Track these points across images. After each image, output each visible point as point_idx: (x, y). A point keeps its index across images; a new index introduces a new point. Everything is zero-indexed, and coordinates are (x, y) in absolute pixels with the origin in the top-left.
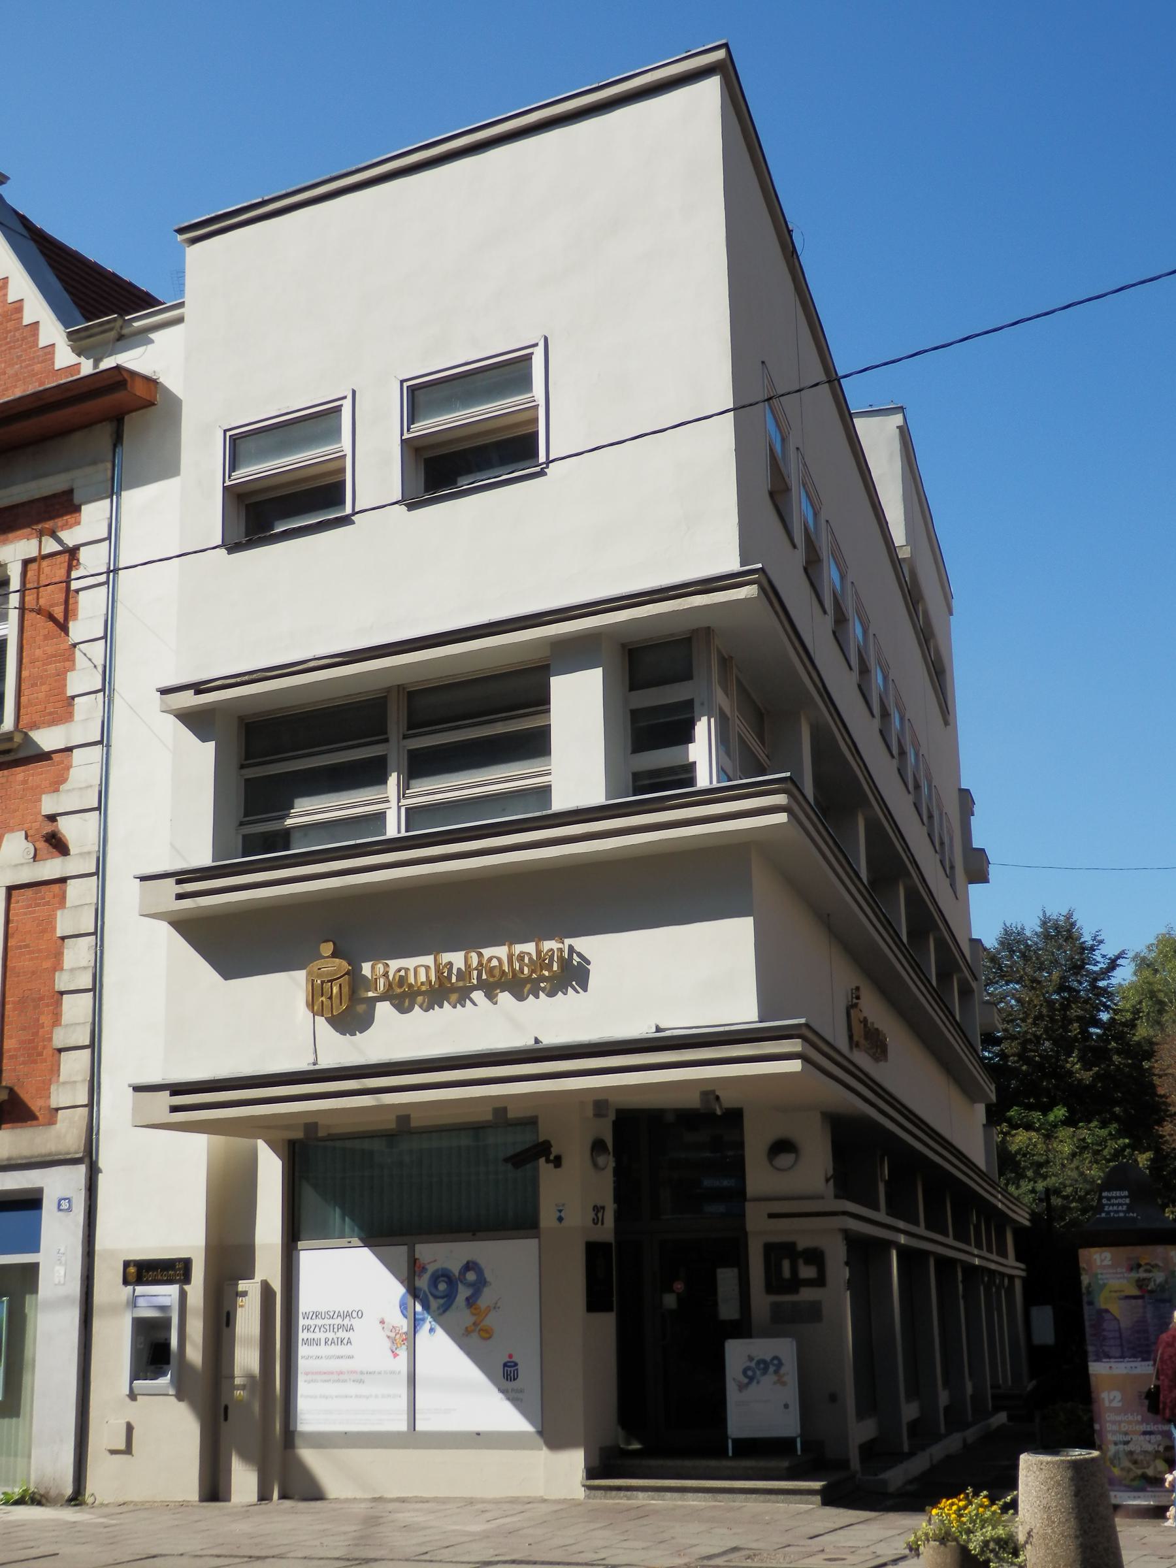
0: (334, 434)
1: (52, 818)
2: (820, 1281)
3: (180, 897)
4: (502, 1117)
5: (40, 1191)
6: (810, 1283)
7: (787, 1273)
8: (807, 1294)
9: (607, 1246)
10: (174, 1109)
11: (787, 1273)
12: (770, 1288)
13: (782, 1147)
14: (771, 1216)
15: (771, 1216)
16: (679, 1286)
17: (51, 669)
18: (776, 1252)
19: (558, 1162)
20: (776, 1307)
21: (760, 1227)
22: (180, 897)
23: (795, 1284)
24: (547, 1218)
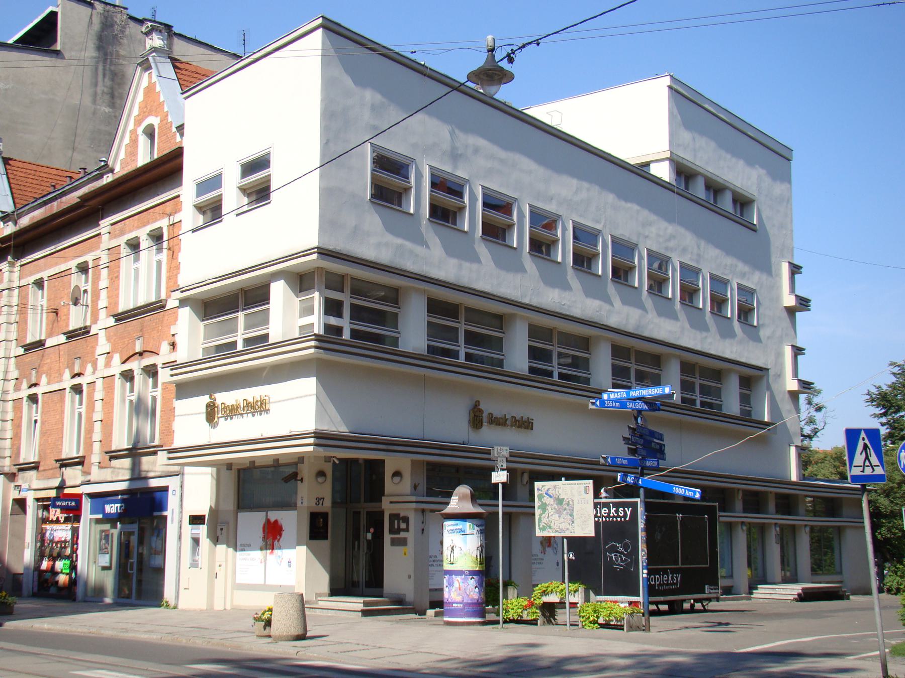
0: (219, 186)
1: (173, 335)
2: (407, 530)
3: (172, 375)
4: (276, 463)
5: (168, 487)
6: (404, 530)
7: (396, 526)
8: (403, 535)
9: (325, 515)
10: (170, 459)
11: (396, 526)
12: (392, 531)
13: (397, 474)
14: (391, 502)
15: (391, 502)
16: (372, 530)
17: (175, 272)
18: (394, 517)
19: (302, 480)
20: (392, 539)
21: (387, 507)
22: (172, 375)
23: (399, 531)
24: (299, 504)
